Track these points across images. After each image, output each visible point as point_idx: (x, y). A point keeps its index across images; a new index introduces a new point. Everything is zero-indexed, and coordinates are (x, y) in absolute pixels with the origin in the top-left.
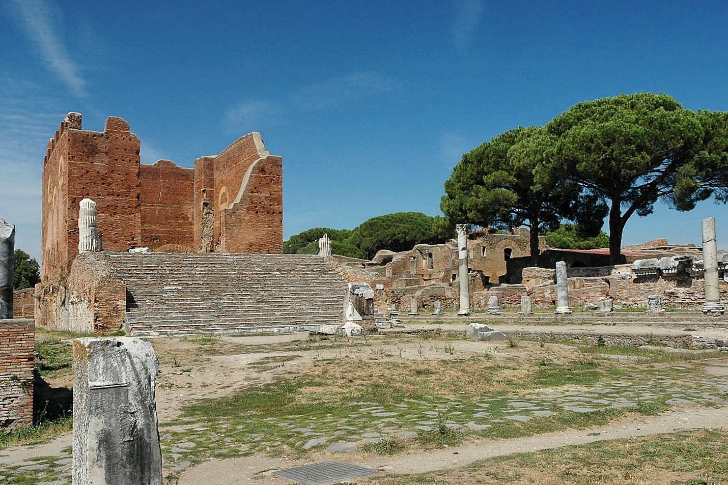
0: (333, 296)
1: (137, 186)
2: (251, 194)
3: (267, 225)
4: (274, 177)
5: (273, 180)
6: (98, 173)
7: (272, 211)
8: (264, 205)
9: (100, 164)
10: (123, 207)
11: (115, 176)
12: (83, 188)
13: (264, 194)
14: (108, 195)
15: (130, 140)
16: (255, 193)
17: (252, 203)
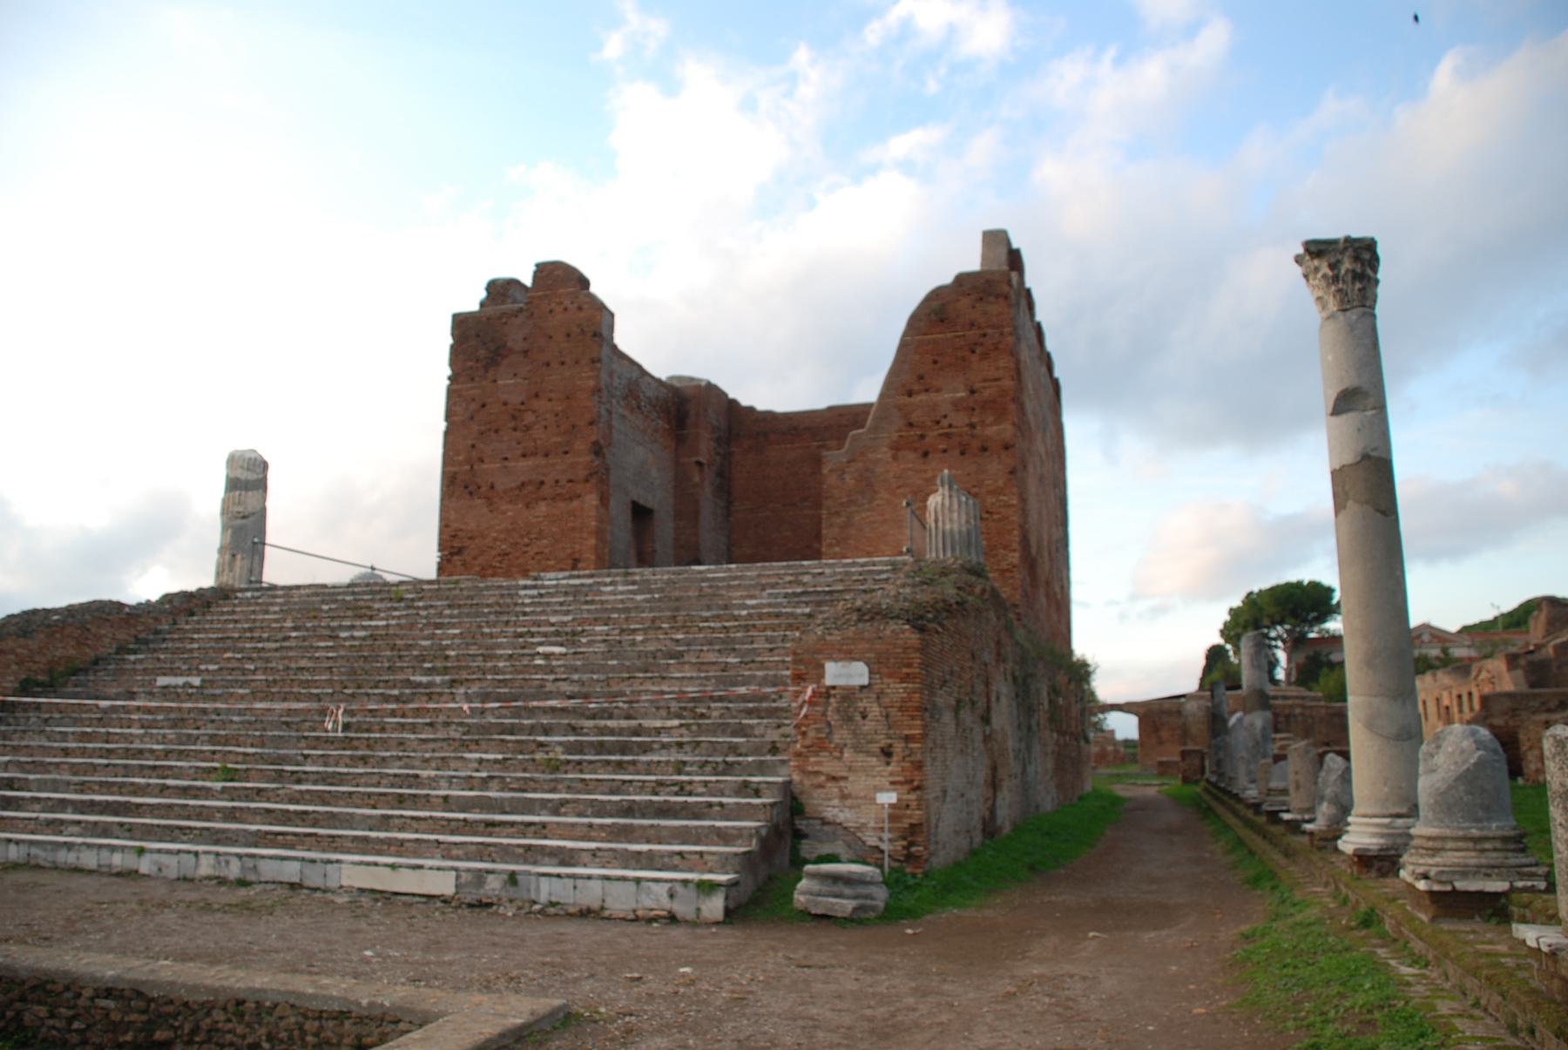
0: (658, 724)
1: (591, 423)
2: (906, 399)
6: (505, 404)
7: (976, 444)
9: (509, 384)
11: (541, 405)
13: (951, 392)
14: (524, 456)
15: (580, 309)
16: (918, 393)
17: (911, 425)
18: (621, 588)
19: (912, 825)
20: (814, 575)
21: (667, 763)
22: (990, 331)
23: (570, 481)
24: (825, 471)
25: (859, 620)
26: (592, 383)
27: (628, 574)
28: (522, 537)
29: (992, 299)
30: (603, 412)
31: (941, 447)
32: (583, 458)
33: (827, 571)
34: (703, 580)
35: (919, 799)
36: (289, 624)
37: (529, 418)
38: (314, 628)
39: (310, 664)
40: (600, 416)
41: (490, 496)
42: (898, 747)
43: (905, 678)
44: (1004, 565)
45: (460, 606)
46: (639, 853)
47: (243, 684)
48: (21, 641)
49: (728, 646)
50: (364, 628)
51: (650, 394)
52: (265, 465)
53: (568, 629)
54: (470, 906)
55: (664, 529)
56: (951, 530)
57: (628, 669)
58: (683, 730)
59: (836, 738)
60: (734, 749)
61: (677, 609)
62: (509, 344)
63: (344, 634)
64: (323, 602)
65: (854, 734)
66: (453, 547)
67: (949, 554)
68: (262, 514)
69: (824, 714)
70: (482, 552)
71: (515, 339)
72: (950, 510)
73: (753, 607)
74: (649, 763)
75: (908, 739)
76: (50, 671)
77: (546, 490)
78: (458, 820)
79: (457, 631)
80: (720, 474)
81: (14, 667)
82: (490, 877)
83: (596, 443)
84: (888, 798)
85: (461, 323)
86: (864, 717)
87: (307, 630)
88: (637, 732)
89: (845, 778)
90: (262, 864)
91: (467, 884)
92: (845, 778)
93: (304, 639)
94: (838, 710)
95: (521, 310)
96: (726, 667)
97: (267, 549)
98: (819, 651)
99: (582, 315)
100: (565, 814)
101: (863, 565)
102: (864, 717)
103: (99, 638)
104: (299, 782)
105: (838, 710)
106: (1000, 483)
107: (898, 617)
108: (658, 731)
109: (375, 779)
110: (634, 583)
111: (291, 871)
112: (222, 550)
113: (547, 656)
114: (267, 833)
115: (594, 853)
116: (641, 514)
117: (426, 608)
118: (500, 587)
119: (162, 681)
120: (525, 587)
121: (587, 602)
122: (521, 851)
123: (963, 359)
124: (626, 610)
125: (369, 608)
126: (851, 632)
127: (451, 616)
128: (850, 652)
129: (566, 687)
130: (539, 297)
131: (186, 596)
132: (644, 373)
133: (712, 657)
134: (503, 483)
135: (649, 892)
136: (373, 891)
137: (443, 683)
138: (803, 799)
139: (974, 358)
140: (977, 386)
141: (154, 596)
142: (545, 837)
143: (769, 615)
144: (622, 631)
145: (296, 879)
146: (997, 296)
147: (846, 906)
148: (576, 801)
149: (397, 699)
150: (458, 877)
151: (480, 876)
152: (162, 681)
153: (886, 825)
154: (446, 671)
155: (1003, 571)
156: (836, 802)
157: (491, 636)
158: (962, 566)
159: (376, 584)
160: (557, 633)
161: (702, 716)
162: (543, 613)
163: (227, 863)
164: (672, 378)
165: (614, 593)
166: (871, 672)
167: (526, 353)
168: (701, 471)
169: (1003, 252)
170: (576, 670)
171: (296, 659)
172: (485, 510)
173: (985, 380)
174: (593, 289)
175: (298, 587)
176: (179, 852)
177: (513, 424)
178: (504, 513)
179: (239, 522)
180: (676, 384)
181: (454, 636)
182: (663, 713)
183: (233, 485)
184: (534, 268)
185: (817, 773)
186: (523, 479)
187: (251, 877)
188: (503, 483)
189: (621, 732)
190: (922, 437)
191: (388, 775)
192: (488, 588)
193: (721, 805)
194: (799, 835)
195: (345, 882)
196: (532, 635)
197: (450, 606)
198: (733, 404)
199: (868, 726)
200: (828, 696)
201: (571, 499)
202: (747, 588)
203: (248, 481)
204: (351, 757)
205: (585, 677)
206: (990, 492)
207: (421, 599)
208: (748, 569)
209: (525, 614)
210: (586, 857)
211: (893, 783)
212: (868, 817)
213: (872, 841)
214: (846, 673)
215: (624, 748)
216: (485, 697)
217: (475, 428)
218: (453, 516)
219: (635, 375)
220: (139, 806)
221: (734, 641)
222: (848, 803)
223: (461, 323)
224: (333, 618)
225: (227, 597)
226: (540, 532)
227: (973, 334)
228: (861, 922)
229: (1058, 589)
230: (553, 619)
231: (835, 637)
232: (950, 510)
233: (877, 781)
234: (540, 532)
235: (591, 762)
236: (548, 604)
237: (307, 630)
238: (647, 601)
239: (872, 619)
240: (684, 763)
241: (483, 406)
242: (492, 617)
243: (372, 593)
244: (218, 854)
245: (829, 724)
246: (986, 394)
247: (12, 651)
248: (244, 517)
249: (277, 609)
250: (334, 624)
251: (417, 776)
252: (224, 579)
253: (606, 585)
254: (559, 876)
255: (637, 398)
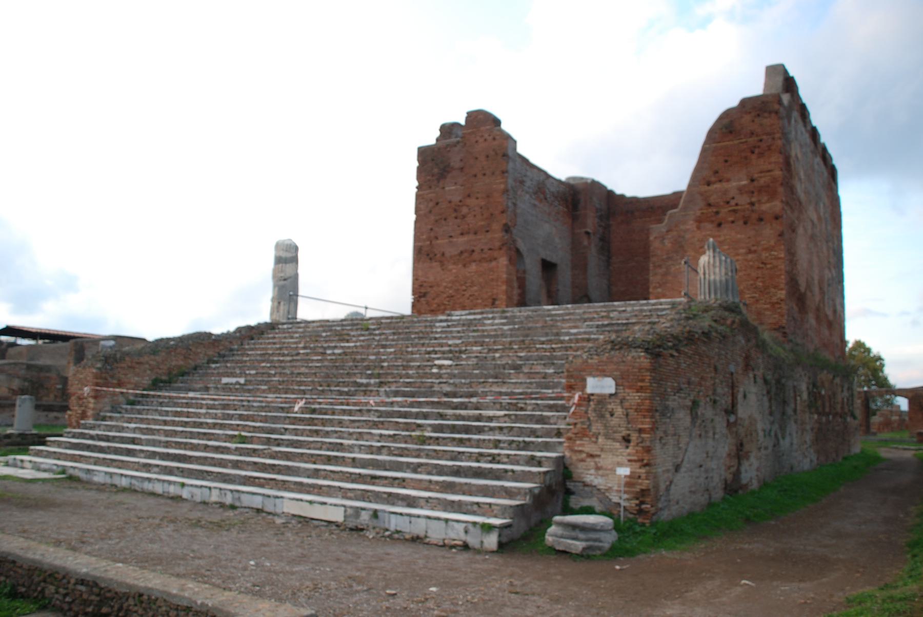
1: (503, 212)
2: (706, 188)
3: (743, 248)
4: (761, 140)
5: (759, 147)
6: (450, 202)
7: (755, 216)
8: (737, 205)
9: (452, 189)
10: (482, 250)
11: (472, 202)
12: (431, 229)
13: (738, 181)
14: (462, 234)
15: (494, 139)
16: (714, 183)
17: (709, 205)
18: (497, 321)
19: (642, 490)
20: (620, 312)
21: (489, 440)
22: (765, 137)
23: (490, 249)
24: (651, 238)
25: (612, 349)
26: (502, 186)
27: (504, 312)
28: (462, 285)
29: (766, 115)
30: (510, 204)
31: (731, 219)
32: (497, 235)
33: (629, 309)
34: (548, 316)
35: (648, 473)
36: (301, 345)
37: (465, 210)
38: (315, 348)
39: (307, 371)
40: (508, 207)
41: (442, 260)
42: (634, 437)
43: (640, 389)
44: (774, 299)
45: (400, 334)
46: (453, 502)
47: (266, 383)
48: (152, 357)
49: (550, 361)
50: (342, 347)
51: (552, 189)
52: (296, 248)
53: (457, 349)
54: (351, 529)
55: (565, 276)
56: (715, 281)
57: (486, 377)
58: (506, 419)
59: (594, 429)
60: (533, 433)
61: (527, 336)
62: (452, 164)
63: (329, 352)
64: (324, 331)
65: (605, 426)
66: (422, 293)
67: (713, 296)
68: (296, 277)
69: (586, 412)
70: (438, 296)
71: (455, 162)
72: (714, 266)
73: (575, 334)
74: (479, 440)
75: (641, 431)
76: (169, 373)
77: (476, 256)
78: (355, 474)
79: (392, 350)
80: (602, 239)
81: (149, 372)
82: (363, 512)
83: (505, 225)
84: (624, 471)
85: (423, 153)
86: (612, 415)
87: (311, 348)
88: (479, 418)
89: (599, 456)
90: (243, 497)
91: (351, 516)
92: (599, 456)
93: (307, 354)
94: (595, 410)
95: (458, 142)
96: (545, 376)
97: (300, 299)
98: (584, 370)
99: (496, 143)
100: (420, 473)
101: (654, 305)
102: (612, 415)
103: (197, 354)
104: (278, 445)
105: (595, 410)
106: (772, 243)
107: (639, 347)
108: (490, 419)
109: (319, 445)
110: (506, 318)
111: (257, 502)
112: (273, 300)
113: (440, 367)
114: (251, 477)
115: (427, 500)
116: (548, 267)
117: (380, 335)
118: (426, 321)
119: (225, 380)
120: (441, 321)
121: (474, 331)
122: (385, 496)
123: (746, 158)
124: (496, 336)
125: (348, 335)
126: (604, 358)
127: (393, 340)
128: (604, 371)
129: (447, 388)
130: (469, 134)
131: (249, 328)
132: (548, 176)
133: (539, 369)
134: (450, 251)
135: (453, 528)
136: (300, 517)
137: (375, 383)
138: (572, 468)
139: (754, 157)
140: (756, 176)
141: (232, 329)
142: (404, 487)
143: (583, 340)
144: (490, 350)
145: (260, 507)
146: (770, 112)
147: (578, 546)
148: (427, 464)
149: (347, 393)
150: (345, 511)
151: (358, 510)
152: (225, 380)
153: (622, 489)
154: (379, 376)
155: (773, 304)
156: (592, 471)
157: (412, 353)
158: (720, 305)
159: (357, 319)
160: (450, 352)
161: (522, 409)
162: (446, 338)
163: (225, 494)
164: (569, 179)
165: (492, 325)
166: (617, 385)
167: (462, 169)
168: (589, 238)
169: (780, 80)
170: (453, 376)
171: (299, 367)
172: (439, 269)
173: (761, 172)
174: (504, 126)
175: (313, 322)
176: (201, 487)
177: (454, 215)
178: (450, 270)
179: (282, 283)
180: (572, 182)
181: (391, 353)
182: (498, 406)
183: (279, 260)
184: (465, 115)
185: (581, 452)
186: (461, 249)
187: (237, 504)
188: (450, 251)
189: (468, 418)
190: (717, 213)
191: (326, 443)
192: (419, 322)
193: (513, 471)
194: (569, 492)
195: (285, 510)
196: (436, 353)
197: (394, 334)
198: (610, 193)
199: (614, 421)
200: (589, 400)
201: (491, 261)
202: (575, 320)
203: (287, 258)
204: (310, 430)
205: (457, 381)
206: (766, 249)
207: (378, 329)
208: (579, 308)
209: (436, 339)
210: (422, 502)
211: (630, 461)
212: (613, 484)
213: (615, 499)
214: (600, 385)
215: (467, 430)
216: (396, 394)
217: (432, 218)
218: (420, 273)
219: (542, 178)
220: (190, 457)
221: (556, 358)
222: (601, 472)
223: (423, 153)
224: (326, 341)
225: (273, 328)
226: (472, 282)
227: (752, 140)
228: (588, 557)
229: (829, 312)
230: (450, 342)
231: (595, 360)
232: (714, 266)
233: (619, 459)
234: (472, 282)
235: (444, 438)
236: (451, 332)
237: (311, 348)
238: (511, 330)
239: (621, 348)
240: (499, 441)
241: (437, 204)
242: (416, 341)
243: (353, 325)
244: (221, 489)
245: (589, 419)
246: (762, 181)
247: (147, 363)
248: (285, 280)
249: (297, 335)
250: (326, 345)
251: (341, 444)
252: (274, 317)
253: (489, 319)
254: (401, 514)
255: (544, 193)
